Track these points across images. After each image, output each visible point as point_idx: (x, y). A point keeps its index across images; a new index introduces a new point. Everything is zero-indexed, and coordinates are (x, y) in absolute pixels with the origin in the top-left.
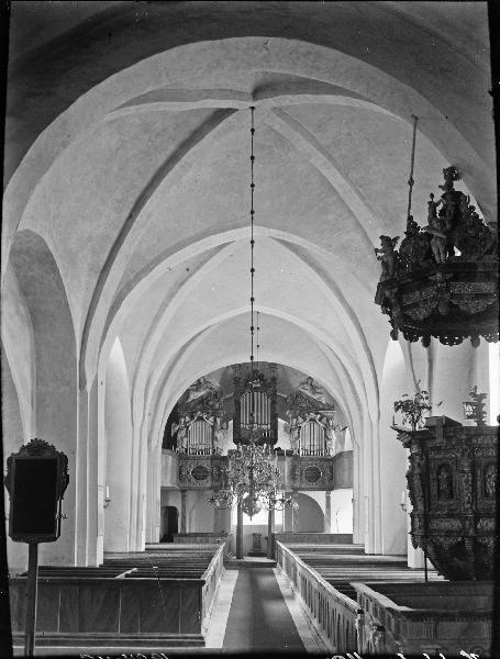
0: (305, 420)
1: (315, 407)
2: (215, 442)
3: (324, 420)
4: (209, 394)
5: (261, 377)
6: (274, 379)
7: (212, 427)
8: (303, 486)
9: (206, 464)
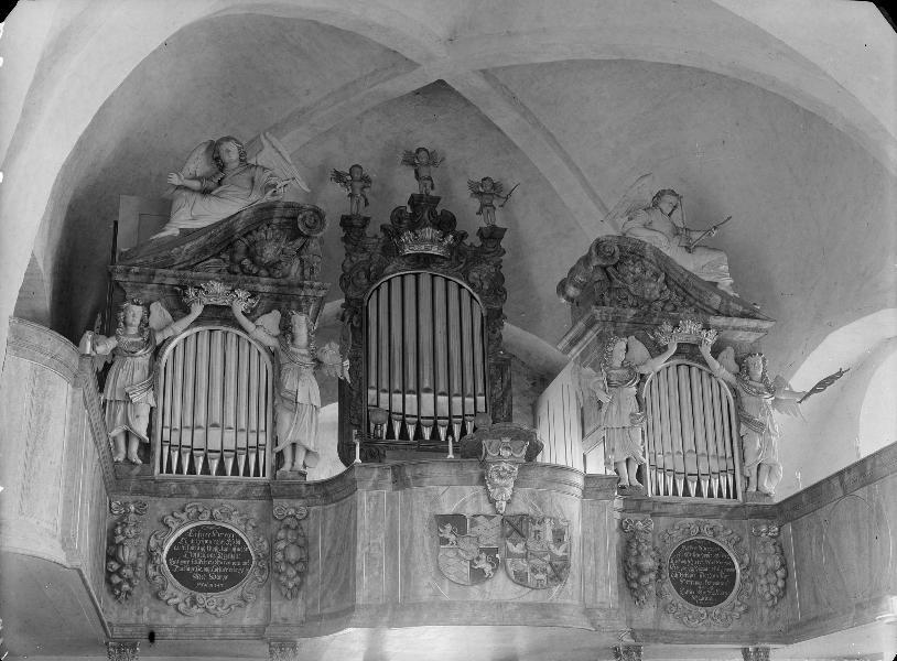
0: (657, 350)
1: (688, 295)
2: (285, 418)
3: (728, 355)
4: (263, 214)
5: (446, 223)
6: (492, 235)
7: (273, 354)
8: (669, 624)
9: (239, 519)
